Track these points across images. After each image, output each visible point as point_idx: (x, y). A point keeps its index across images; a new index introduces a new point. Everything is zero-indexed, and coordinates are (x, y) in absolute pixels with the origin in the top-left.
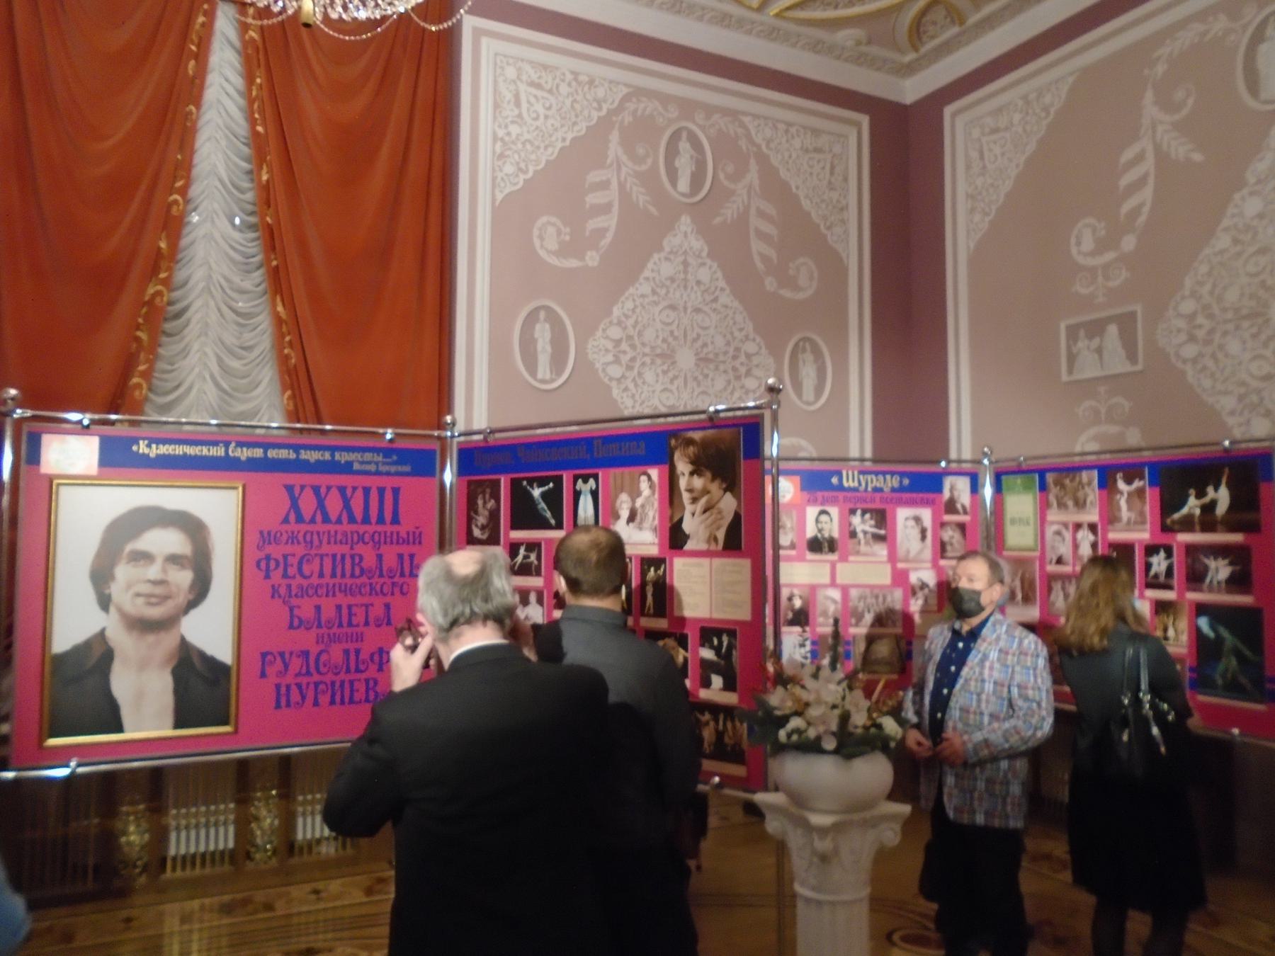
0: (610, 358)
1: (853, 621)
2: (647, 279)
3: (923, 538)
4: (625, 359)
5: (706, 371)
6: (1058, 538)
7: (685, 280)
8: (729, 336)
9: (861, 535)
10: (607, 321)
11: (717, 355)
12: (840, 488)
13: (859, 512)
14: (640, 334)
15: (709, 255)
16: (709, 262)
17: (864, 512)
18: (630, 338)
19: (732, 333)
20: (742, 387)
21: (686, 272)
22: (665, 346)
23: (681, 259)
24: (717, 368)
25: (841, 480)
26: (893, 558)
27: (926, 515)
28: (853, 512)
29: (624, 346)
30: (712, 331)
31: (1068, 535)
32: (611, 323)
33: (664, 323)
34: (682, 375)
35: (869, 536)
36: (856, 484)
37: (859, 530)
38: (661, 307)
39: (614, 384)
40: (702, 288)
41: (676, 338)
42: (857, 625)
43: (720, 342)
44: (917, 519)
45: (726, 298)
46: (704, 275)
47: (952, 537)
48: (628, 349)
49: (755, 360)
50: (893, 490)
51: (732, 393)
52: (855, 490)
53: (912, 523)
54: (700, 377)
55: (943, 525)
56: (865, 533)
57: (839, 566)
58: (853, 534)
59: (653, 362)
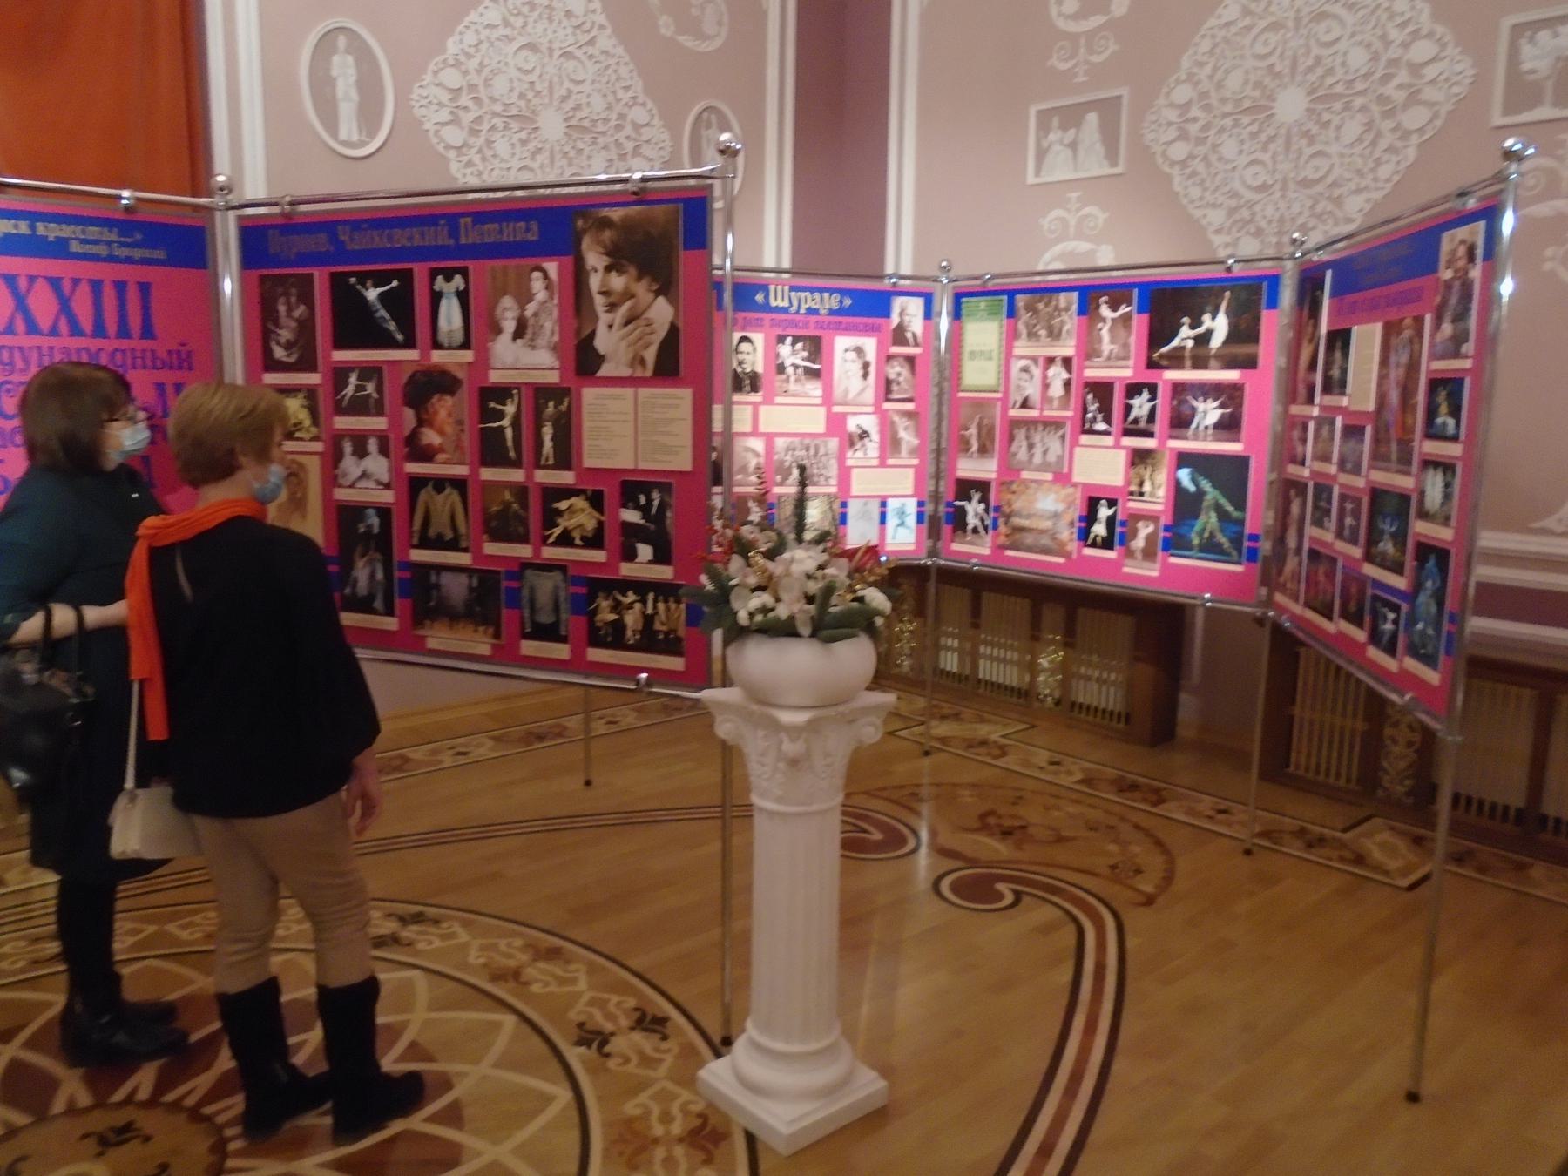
0: (1172, 133)
1: (778, 478)
3: (865, 375)
6: (1025, 376)
9: (790, 370)
12: (767, 308)
13: (789, 340)
14: (1220, 86)
17: (796, 340)
24: (1347, 107)
25: (767, 297)
26: (828, 400)
27: (870, 344)
28: (781, 339)
29: (1195, 112)
31: (1037, 372)
34: (1283, 131)
35: (800, 371)
36: (786, 304)
37: (788, 363)
39: (1176, 171)
42: (781, 484)
43: (1358, 59)
44: (859, 351)
47: (899, 374)
50: (832, 312)
51: (1374, 143)
52: (785, 310)
53: (853, 355)
54: (1315, 130)
55: (890, 358)
56: (796, 367)
57: (763, 409)
58: (781, 369)
59: (1236, 124)
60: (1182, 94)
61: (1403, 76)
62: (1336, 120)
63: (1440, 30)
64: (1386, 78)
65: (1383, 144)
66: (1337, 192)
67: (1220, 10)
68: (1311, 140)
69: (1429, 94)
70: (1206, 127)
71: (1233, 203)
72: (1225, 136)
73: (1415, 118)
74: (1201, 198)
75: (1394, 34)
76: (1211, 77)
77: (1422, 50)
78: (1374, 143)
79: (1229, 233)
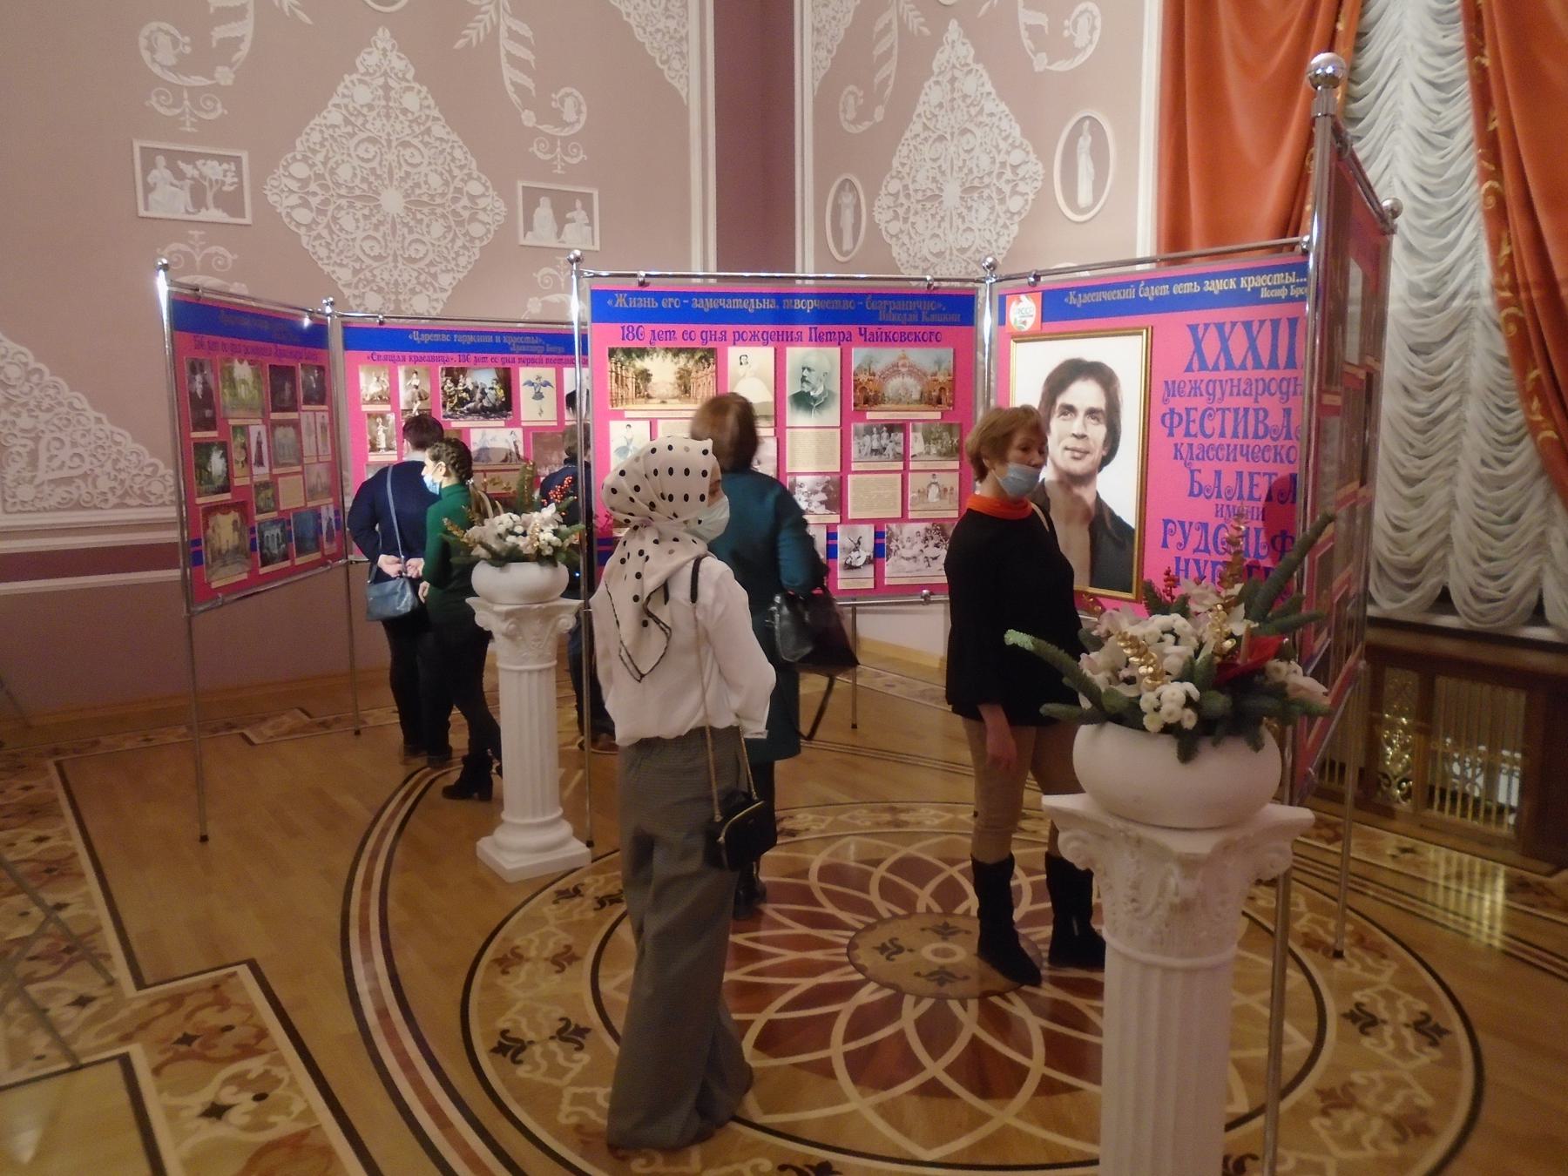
2: (337, 106)
4: (315, 201)
5: (419, 216)
7: (387, 107)
8: (446, 175)
10: (289, 156)
11: (432, 197)
14: (332, 172)
15: (415, 78)
16: (417, 86)
18: (319, 176)
19: (450, 171)
20: (467, 234)
21: (387, 98)
22: (365, 186)
23: (381, 81)
24: (433, 213)
29: (313, 187)
30: (424, 169)
32: (294, 159)
33: (363, 159)
34: (389, 219)
38: (356, 140)
39: (302, 231)
40: (410, 116)
41: (378, 177)
45: (439, 130)
46: (411, 101)
48: (317, 190)
49: (482, 203)
51: (453, 241)
54: (412, 223)
59: (351, 205)
60: (300, 170)
61: (465, 201)
62: (426, 220)
63: (484, 178)
64: (455, 200)
65: (459, 243)
66: (433, 270)
67: (324, 113)
68: (411, 231)
69: (482, 216)
70: (326, 202)
71: (357, 266)
72: (343, 213)
73: (476, 230)
74: (329, 258)
75: (456, 172)
76: (324, 164)
77: (475, 188)
78: (453, 241)
79: (356, 287)
